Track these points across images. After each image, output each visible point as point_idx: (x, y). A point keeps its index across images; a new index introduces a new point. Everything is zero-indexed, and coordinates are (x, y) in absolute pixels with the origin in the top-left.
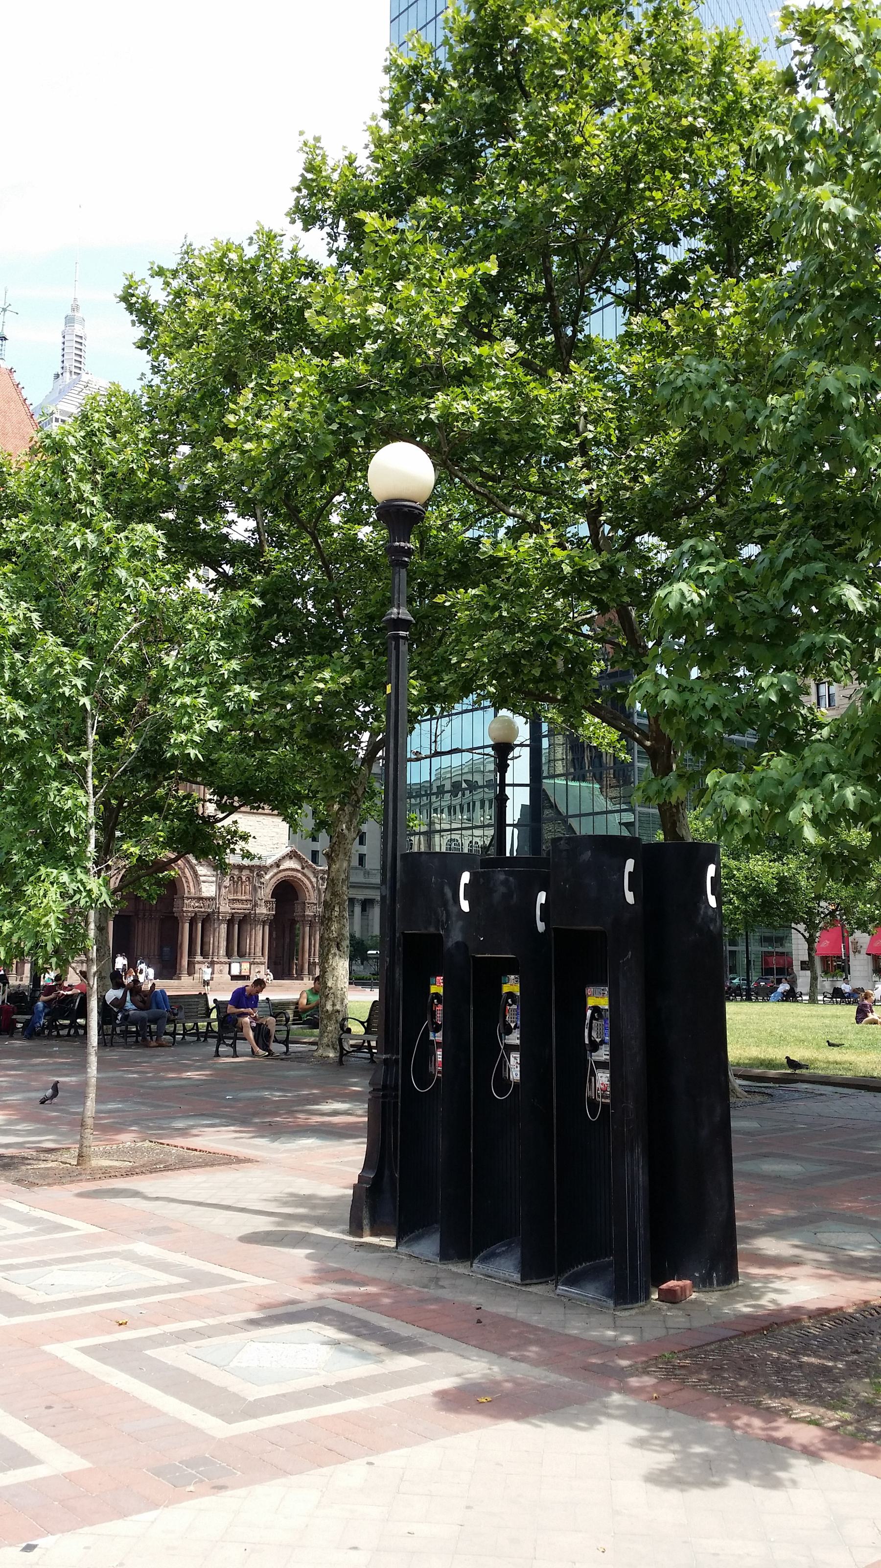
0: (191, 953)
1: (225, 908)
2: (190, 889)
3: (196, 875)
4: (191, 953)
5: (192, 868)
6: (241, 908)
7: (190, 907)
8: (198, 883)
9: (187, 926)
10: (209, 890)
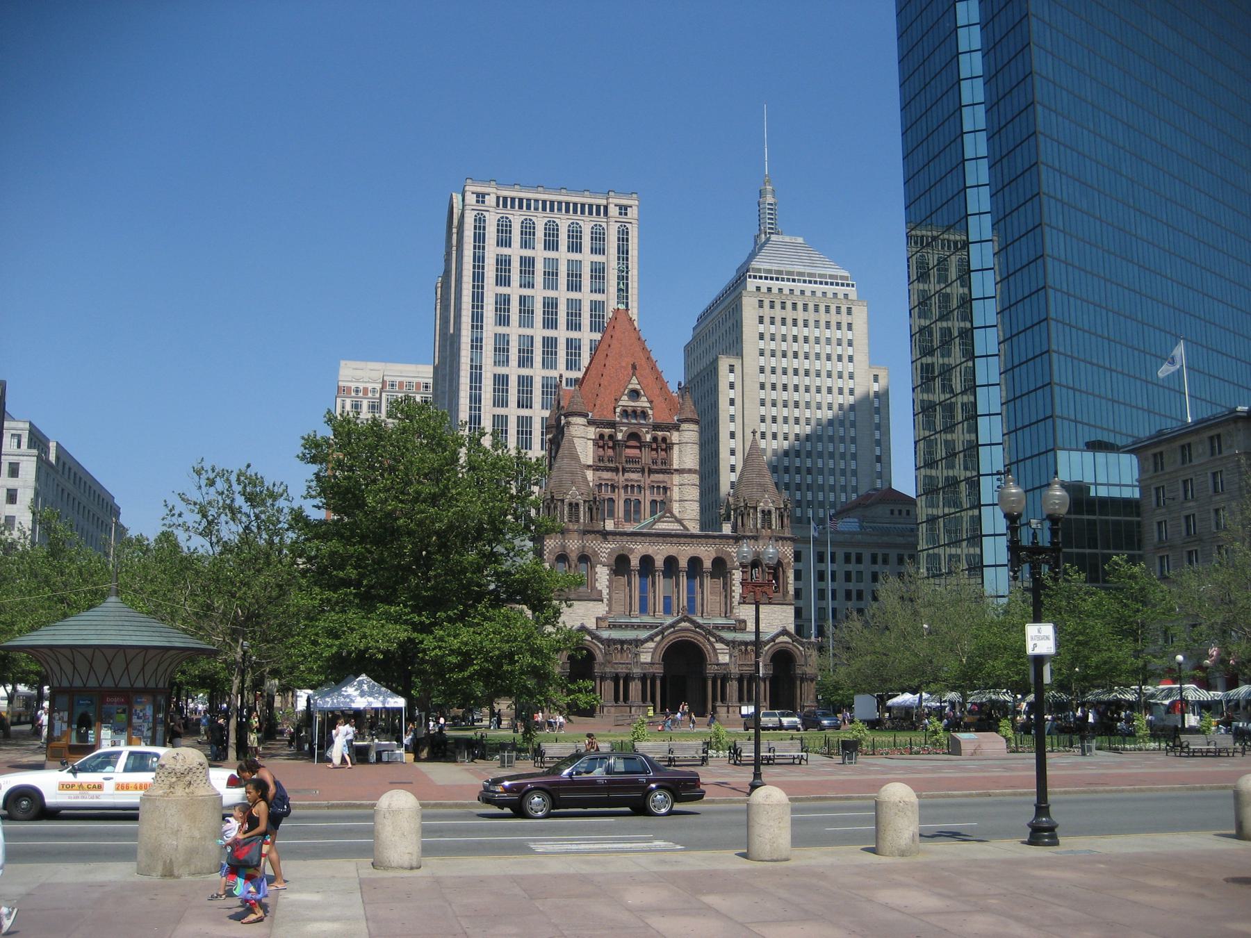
0: (714, 699)
1: (735, 670)
2: (710, 657)
3: (714, 649)
4: (714, 699)
5: (711, 644)
6: (748, 670)
7: (711, 670)
8: (716, 654)
9: (710, 683)
10: (724, 659)
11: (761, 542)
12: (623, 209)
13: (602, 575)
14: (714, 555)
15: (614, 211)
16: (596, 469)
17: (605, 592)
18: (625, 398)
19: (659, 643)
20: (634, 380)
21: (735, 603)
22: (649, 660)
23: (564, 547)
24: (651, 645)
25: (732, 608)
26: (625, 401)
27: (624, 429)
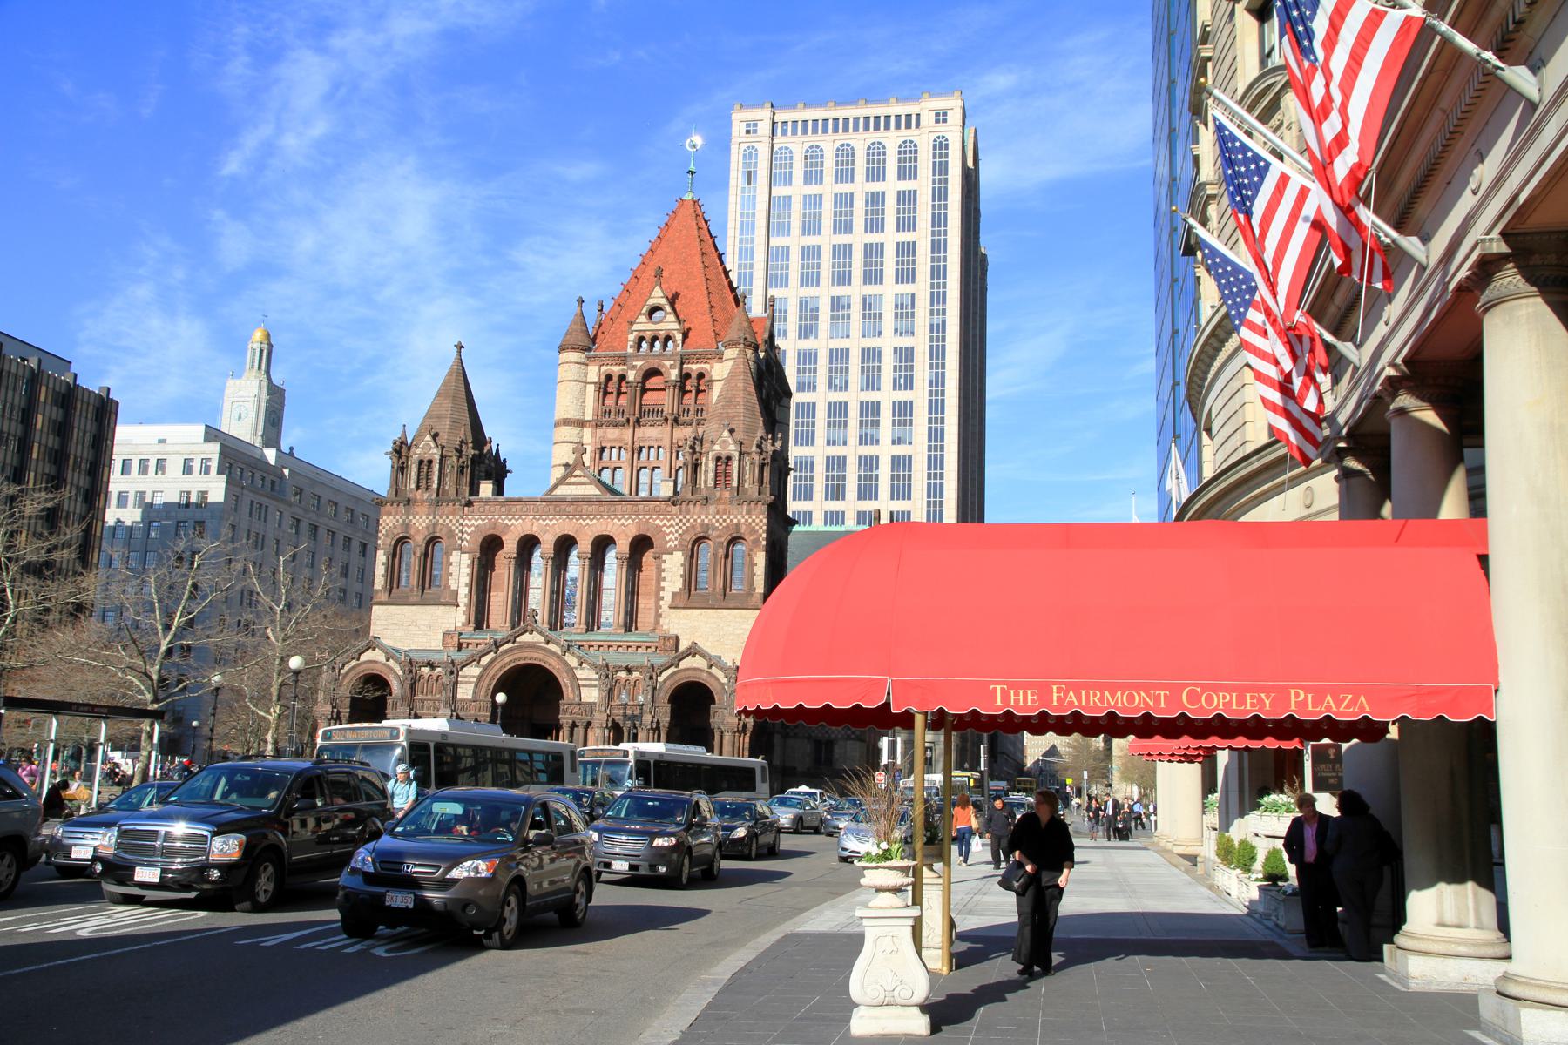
2: (568, 693)
5: (571, 670)
10: (591, 695)
11: (712, 508)
12: (941, 117)
13: (459, 571)
14: (633, 532)
15: (928, 119)
16: (598, 424)
17: (463, 592)
18: (643, 319)
19: (485, 668)
20: (658, 292)
21: (665, 604)
22: (470, 696)
23: (407, 526)
24: (473, 671)
25: (658, 616)
26: (643, 325)
27: (639, 364)
